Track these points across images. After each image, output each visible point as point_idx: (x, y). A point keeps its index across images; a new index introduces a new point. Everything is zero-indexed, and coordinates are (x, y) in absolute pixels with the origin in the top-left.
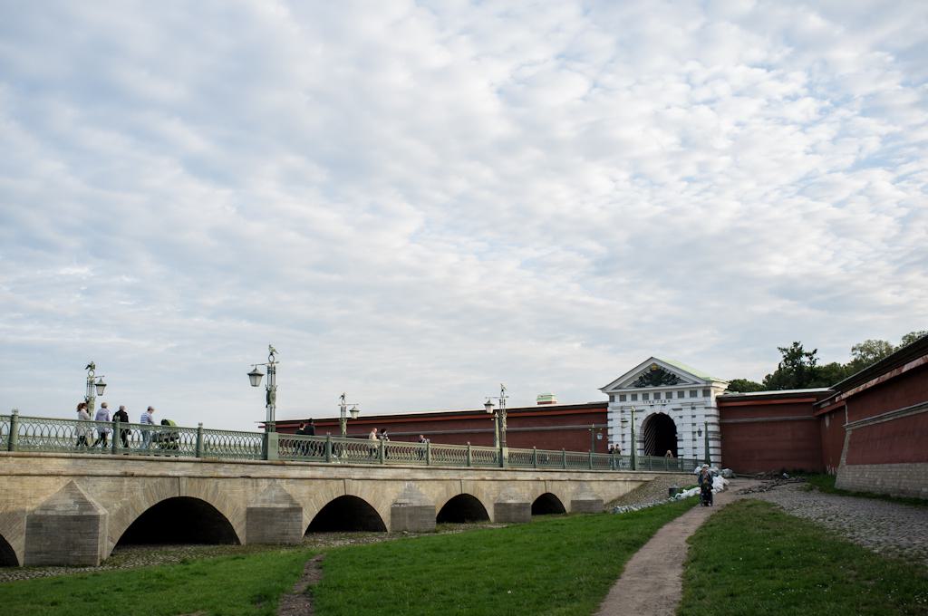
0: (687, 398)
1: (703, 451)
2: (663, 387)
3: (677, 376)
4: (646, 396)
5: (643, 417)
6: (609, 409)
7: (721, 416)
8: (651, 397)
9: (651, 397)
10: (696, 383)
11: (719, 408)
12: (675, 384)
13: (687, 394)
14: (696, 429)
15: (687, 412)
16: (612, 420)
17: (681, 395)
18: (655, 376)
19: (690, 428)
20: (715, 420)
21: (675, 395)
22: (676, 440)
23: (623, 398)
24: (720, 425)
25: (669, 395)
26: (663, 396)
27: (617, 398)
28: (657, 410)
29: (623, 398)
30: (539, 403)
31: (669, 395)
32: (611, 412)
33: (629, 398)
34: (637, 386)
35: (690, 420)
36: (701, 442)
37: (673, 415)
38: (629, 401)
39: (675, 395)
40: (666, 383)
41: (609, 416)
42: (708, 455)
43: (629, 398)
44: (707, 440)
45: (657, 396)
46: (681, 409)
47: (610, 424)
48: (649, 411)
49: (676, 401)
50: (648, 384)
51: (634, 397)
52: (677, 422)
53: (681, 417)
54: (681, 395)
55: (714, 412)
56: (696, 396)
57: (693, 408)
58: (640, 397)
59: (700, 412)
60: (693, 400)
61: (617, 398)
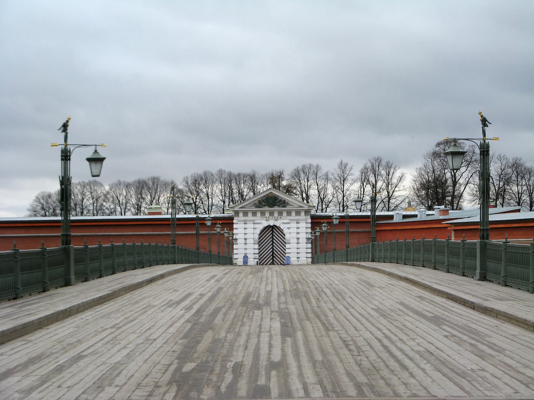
2: (276, 208)
3: (287, 202)
4: (263, 214)
5: (260, 227)
6: (234, 221)
8: (267, 215)
9: (267, 215)
10: (301, 207)
12: (285, 207)
13: (293, 214)
15: (294, 225)
16: (237, 229)
18: (271, 201)
21: (285, 214)
23: (245, 214)
26: (276, 215)
27: (241, 214)
28: (272, 223)
29: (245, 214)
31: (280, 213)
32: (237, 223)
33: (250, 214)
34: (256, 207)
37: (282, 227)
39: (285, 214)
40: (279, 206)
43: (250, 214)
45: (272, 214)
46: (289, 223)
47: (235, 231)
48: (265, 224)
50: (265, 206)
51: (254, 214)
53: (289, 228)
54: (289, 213)
56: (300, 215)
58: (259, 214)
60: (297, 217)
61: (241, 214)
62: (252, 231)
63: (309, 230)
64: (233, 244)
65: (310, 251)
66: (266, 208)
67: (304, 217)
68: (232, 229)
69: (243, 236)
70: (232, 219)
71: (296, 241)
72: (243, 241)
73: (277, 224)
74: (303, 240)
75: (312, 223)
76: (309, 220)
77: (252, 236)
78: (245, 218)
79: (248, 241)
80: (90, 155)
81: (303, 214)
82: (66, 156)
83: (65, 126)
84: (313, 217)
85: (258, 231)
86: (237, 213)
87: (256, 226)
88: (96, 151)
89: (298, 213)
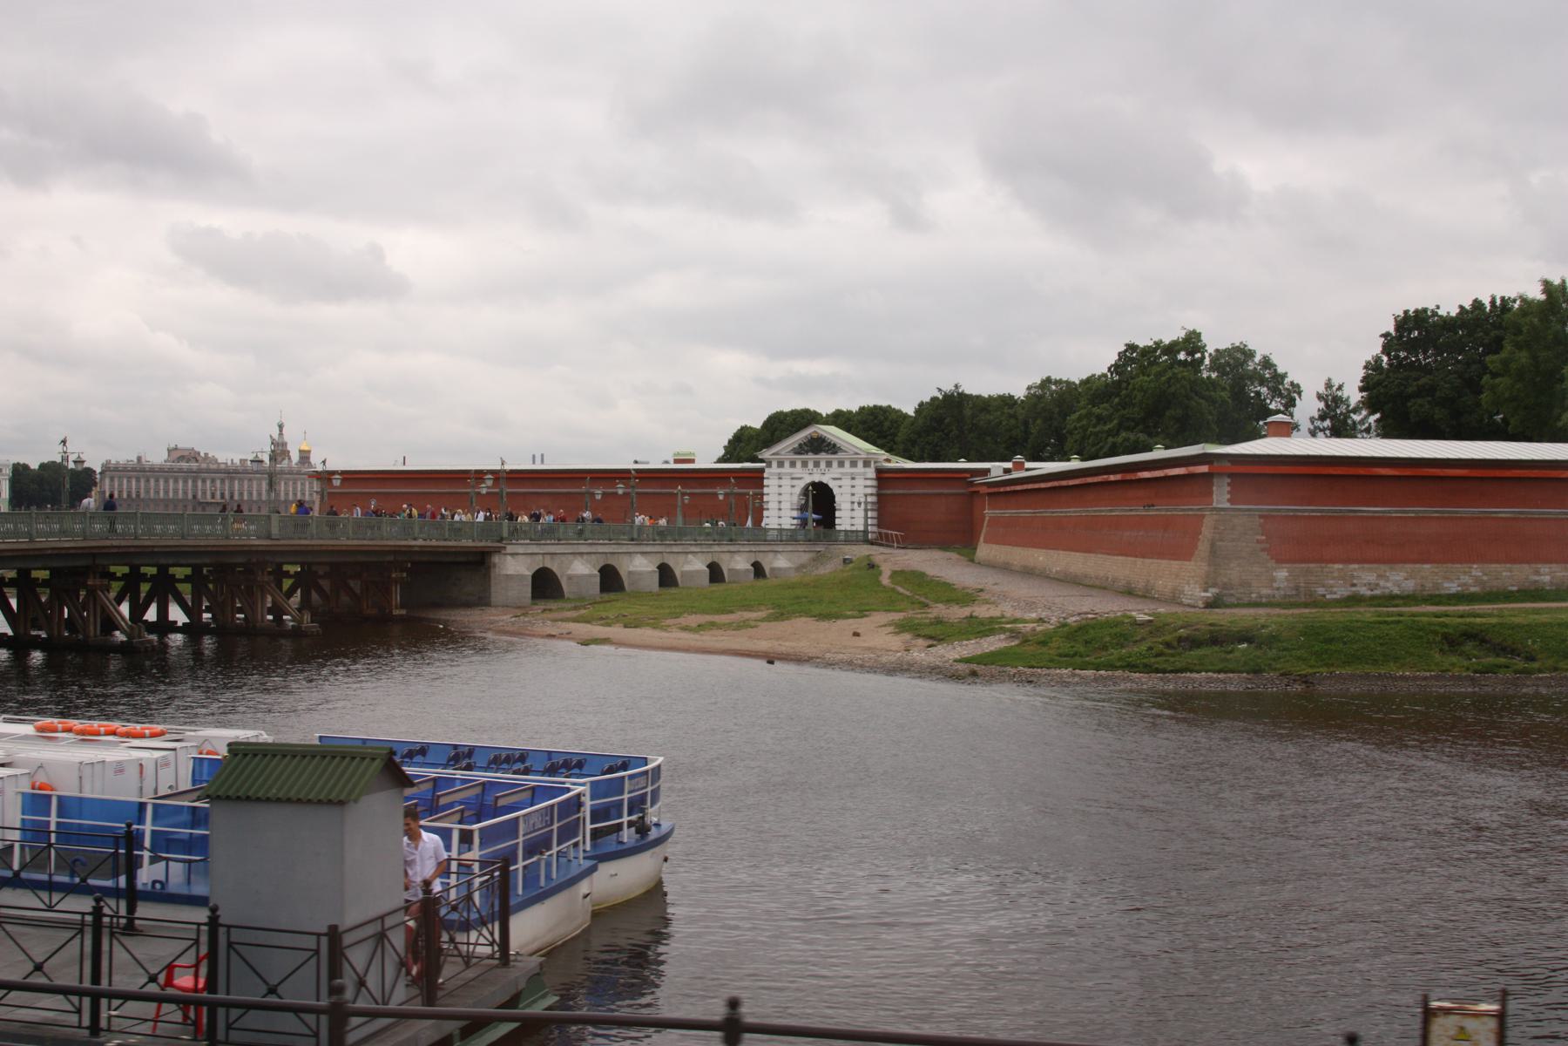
0: (847, 468)
1: (862, 521)
2: (823, 456)
4: (805, 464)
5: (801, 484)
7: (879, 487)
8: (811, 465)
9: (811, 465)
11: (879, 479)
13: (847, 464)
14: (856, 499)
15: (846, 482)
17: (841, 464)
19: (849, 498)
20: (874, 491)
21: (835, 464)
22: (834, 510)
23: (781, 464)
24: (879, 495)
25: (829, 464)
26: (823, 465)
27: (774, 464)
29: (781, 464)
30: (676, 461)
31: (829, 464)
33: (787, 464)
35: (849, 490)
36: (860, 513)
37: (832, 484)
38: (787, 469)
39: (835, 464)
42: (866, 525)
43: (787, 464)
44: (866, 510)
45: (817, 464)
47: (766, 490)
48: (808, 479)
49: (836, 470)
51: (793, 464)
52: (836, 491)
54: (841, 464)
55: (874, 483)
58: (799, 464)
59: (860, 482)
66: (811, 456)
68: (762, 486)
70: (762, 471)
76: (873, 475)
87: (795, 482)
89: (854, 464)
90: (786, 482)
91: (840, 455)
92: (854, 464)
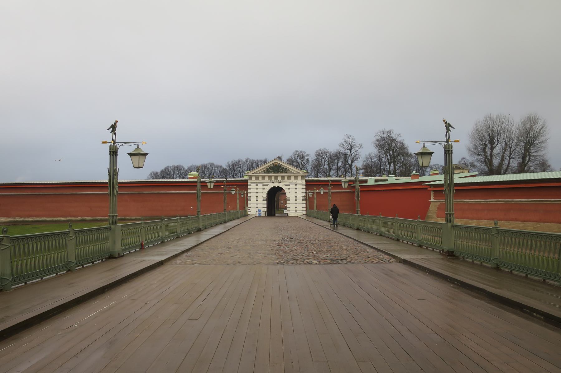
2: (280, 174)
4: (270, 178)
5: (268, 188)
6: (249, 184)
8: (273, 178)
9: (273, 178)
10: (298, 173)
13: (293, 178)
15: (292, 186)
17: (289, 178)
21: (286, 178)
23: (257, 178)
26: (280, 178)
27: (254, 178)
28: (276, 185)
29: (257, 178)
31: (283, 178)
33: (260, 178)
34: (265, 173)
37: (284, 187)
39: (286, 178)
40: (281, 172)
41: (249, 187)
43: (260, 178)
45: (276, 178)
47: (249, 191)
48: (272, 185)
49: (286, 182)
50: (271, 172)
51: (263, 178)
53: (289, 189)
54: (289, 178)
57: (296, 185)
58: (267, 178)
62: (262, 190)
63: (304, 191)
64: (247, 200)
65: (305, 206)
66: (272, 174)
67: (301, 181)
68: (247, 189)
69: (256, 195)
70: (247, 181)
71: (294, 198)
72: (255, 198)
73: (281, 185)
74: (300, 198)
75: (306, 185)
76: (305, 183)
77: (262, 194)
78: (256, 181)
79: (258, 198)
80: (131, 151)
81: (299, 178)
82: (114, 152)
83: (114, 127)
84: (307, 181)
85: (266, 191)
86: (251, 177)
87: (264, 187)
88: (138, 147)
89: (296, 178)
90: (260, 187)
91: (289, 174)
92: (296, 178)
